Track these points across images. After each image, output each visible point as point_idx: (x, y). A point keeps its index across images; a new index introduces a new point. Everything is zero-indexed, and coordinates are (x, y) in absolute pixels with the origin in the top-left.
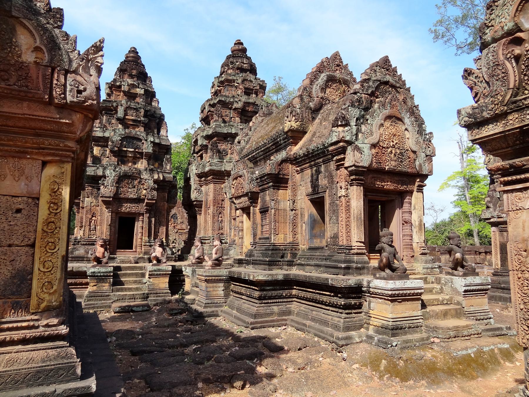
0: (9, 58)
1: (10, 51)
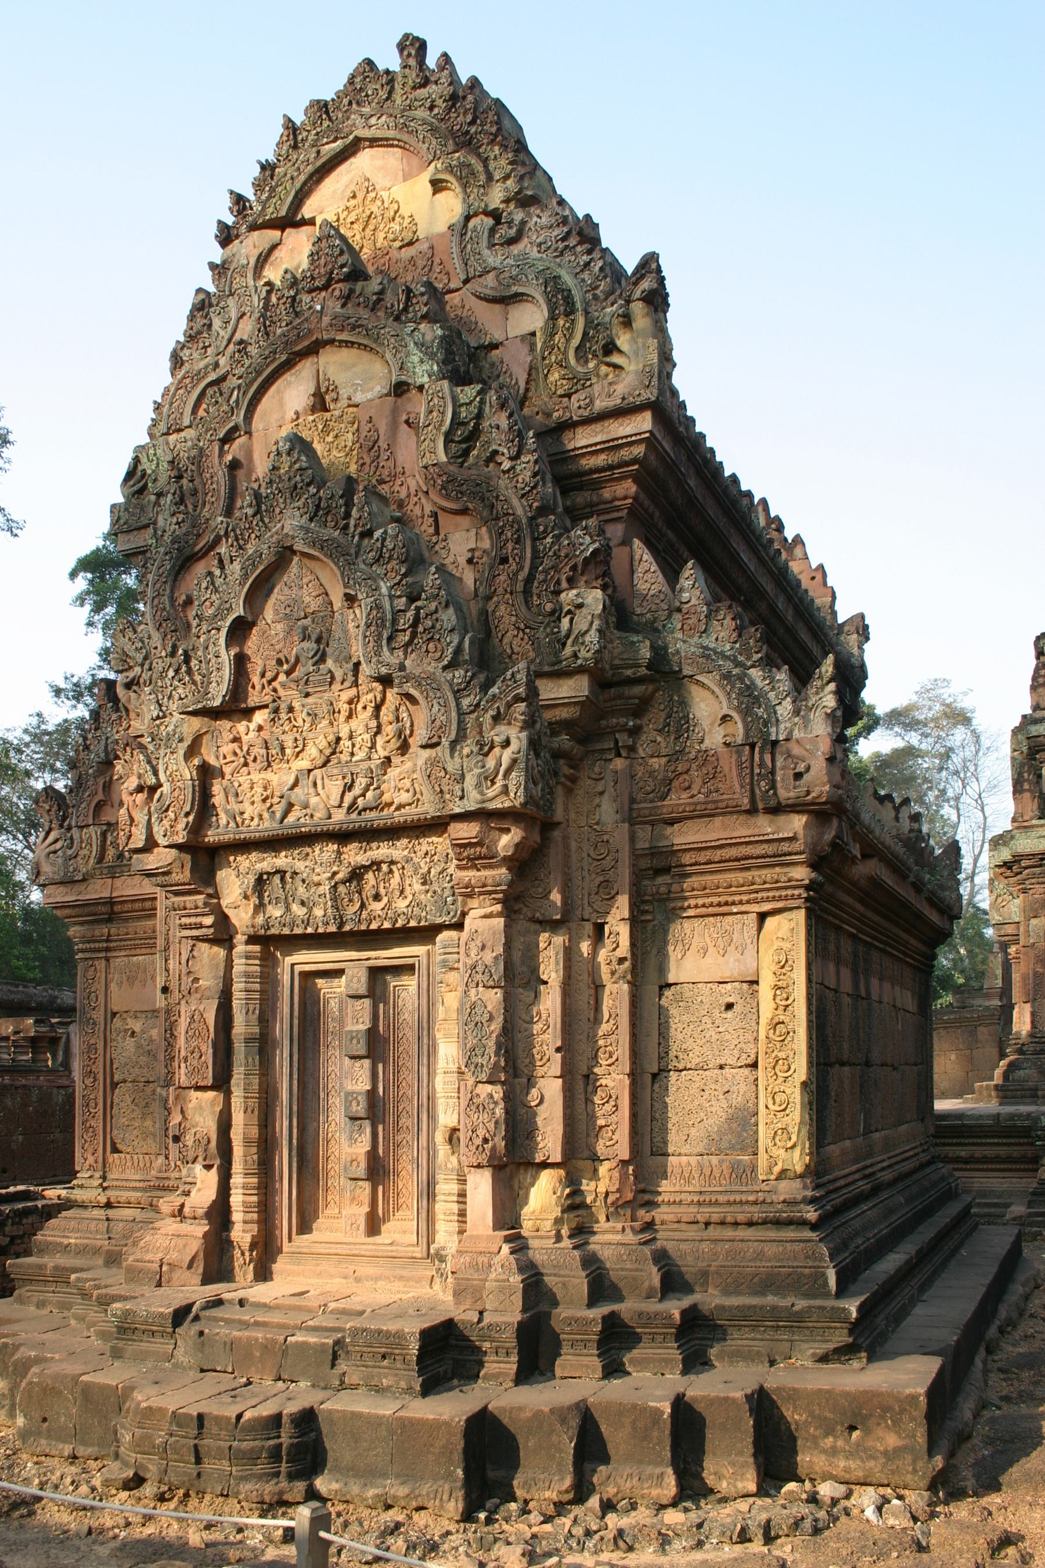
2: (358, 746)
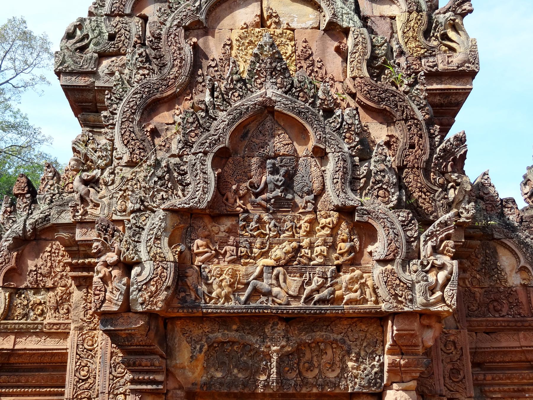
0: (497, 286)
1: (498, 278)
2: (315, 254)
